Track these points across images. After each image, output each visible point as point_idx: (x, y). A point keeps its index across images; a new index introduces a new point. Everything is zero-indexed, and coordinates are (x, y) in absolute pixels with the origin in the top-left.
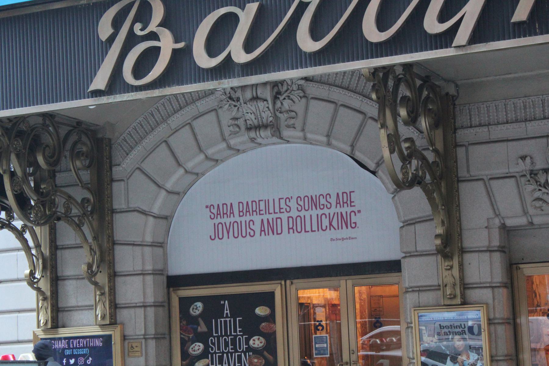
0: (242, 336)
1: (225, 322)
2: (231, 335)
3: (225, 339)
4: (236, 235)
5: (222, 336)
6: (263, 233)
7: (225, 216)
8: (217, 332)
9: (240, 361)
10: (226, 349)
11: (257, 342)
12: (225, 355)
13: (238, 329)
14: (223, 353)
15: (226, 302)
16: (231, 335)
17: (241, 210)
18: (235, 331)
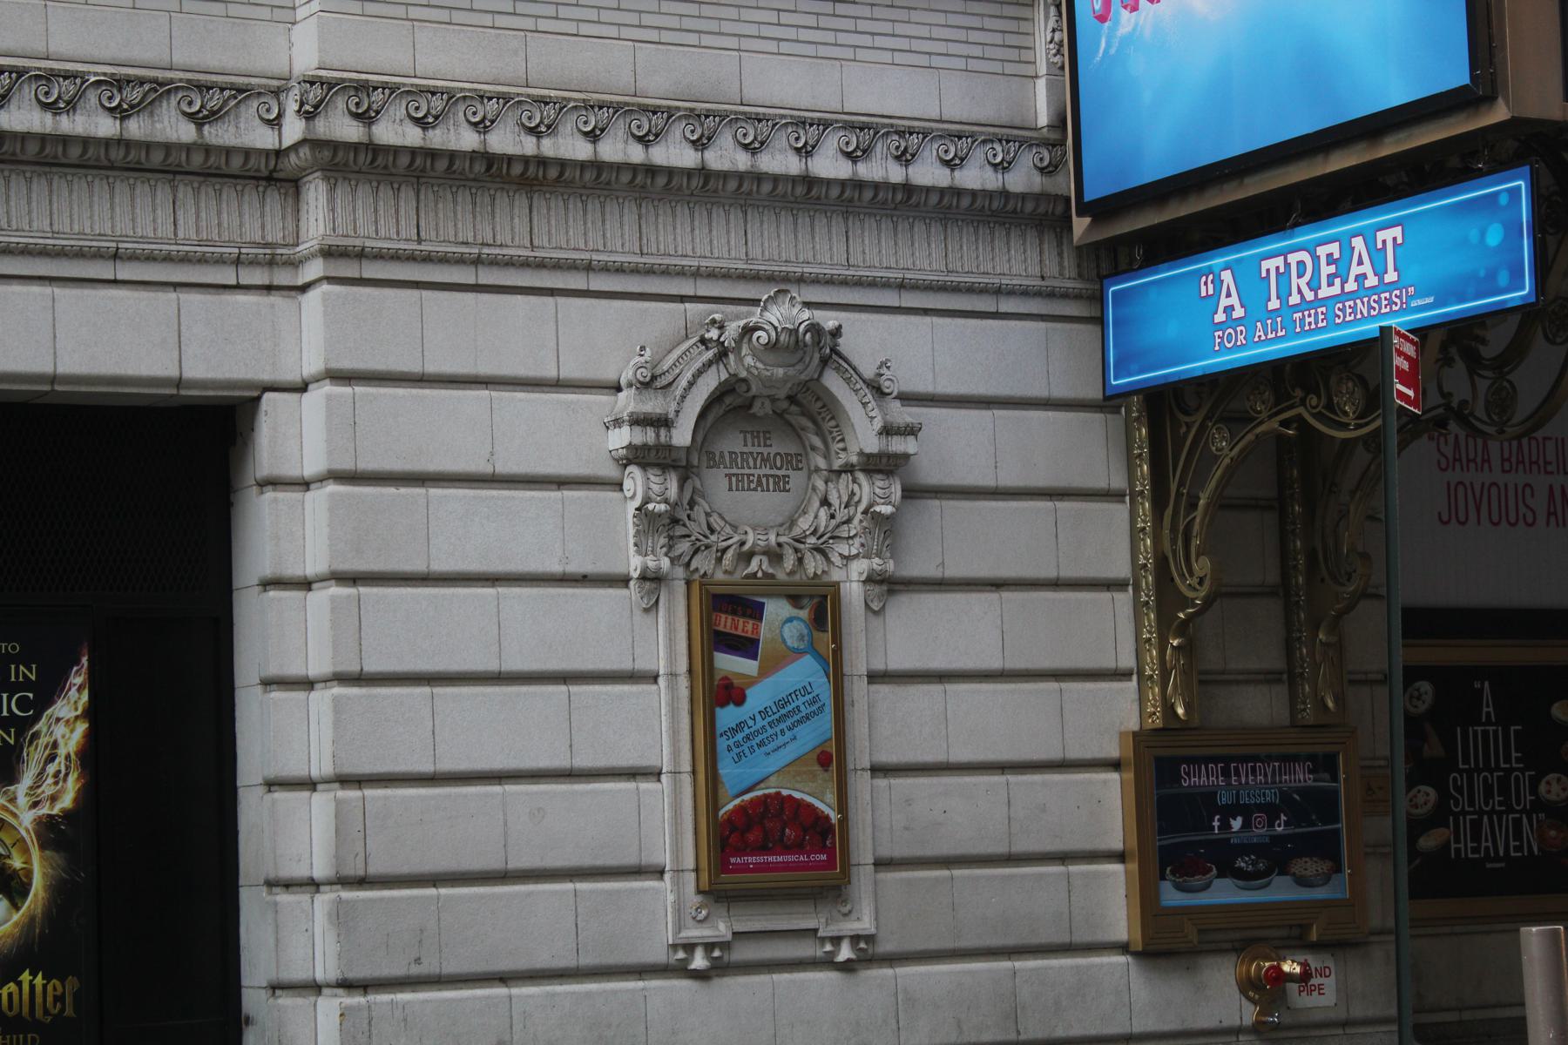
0: (1522, 771)
1: (1485, 733)
2: (1498, 768)
3: (1485, 778)
4: (1495, 518)
5: (1479, 771)
6: (1553, 519)
7: (1472, 465)
8: (1466, 760)
9: (1518, 834)
10: (1487, 804)
11: (1555, 788)
12: (1485, 819)
13: (1514, 755)
14: (1481, 813)
15: (1486, 684)
16: (1498, 768)
17: (1506, 455)
18: (1508, 760)
